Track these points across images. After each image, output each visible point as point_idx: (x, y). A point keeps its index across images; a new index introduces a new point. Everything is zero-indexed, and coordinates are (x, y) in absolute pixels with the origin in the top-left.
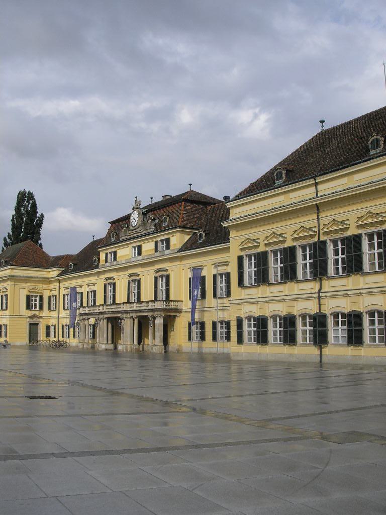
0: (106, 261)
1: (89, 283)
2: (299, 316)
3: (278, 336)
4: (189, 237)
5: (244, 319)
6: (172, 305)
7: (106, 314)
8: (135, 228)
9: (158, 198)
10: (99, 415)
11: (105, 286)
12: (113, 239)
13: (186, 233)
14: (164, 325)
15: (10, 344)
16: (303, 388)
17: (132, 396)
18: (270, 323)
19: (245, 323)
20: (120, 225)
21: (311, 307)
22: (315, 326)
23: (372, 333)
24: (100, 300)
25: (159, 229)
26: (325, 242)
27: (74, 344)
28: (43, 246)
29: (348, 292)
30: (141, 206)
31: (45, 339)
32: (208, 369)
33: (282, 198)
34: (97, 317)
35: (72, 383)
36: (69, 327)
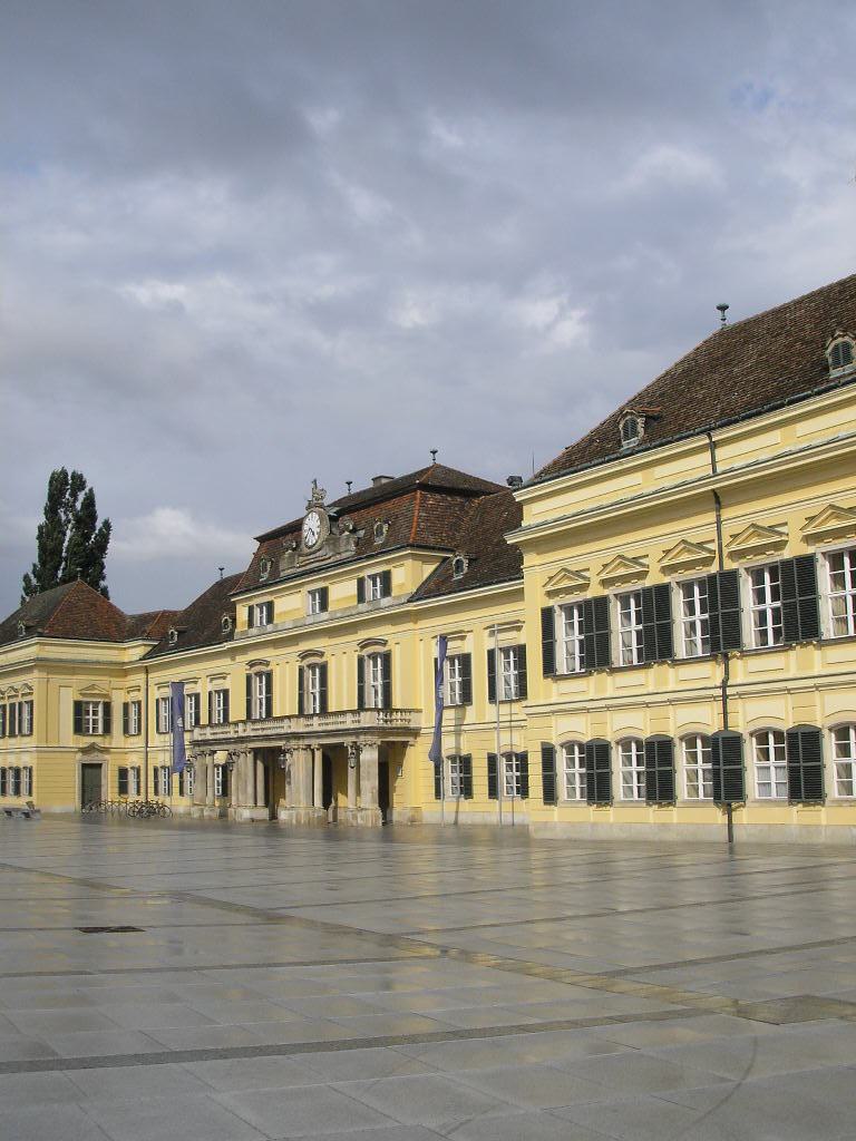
0: (251, 624)
1: (212, 674)
2: (681, 739)
3: (635, 784)
4: (434, 567)
5: (558, 748)
6: (398, 720)
7: (253, 741)
8: (313, 550)
9: (363, 484)
10: (236, 967)
11: (249, 679)
12: (265, 576)
13: (426, 560)
14: (380, 764)
15: (38, 811)
16: (691, 900)
17: (311, 924)
18: (617, 756)
19: (561, 758)
20: (280, 541)
21: (708, 720)
22: (716, 762)
23: (844, 774)
24: (237, 711)
25: (365, 551)
26: (731, 579)
27: (181, 810)
28: (110, 594)
29: (790, 685)
30: (327, 501)
31: (117, 797)
32: (479, 860)
33: (637, 477)
34: (231, 747)
35: (179, 896)
36: (169, 771)
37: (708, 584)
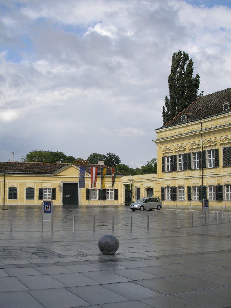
21: (198, 183)
22: (200, 192)
26: (204, 152)
37: (199, 153)
